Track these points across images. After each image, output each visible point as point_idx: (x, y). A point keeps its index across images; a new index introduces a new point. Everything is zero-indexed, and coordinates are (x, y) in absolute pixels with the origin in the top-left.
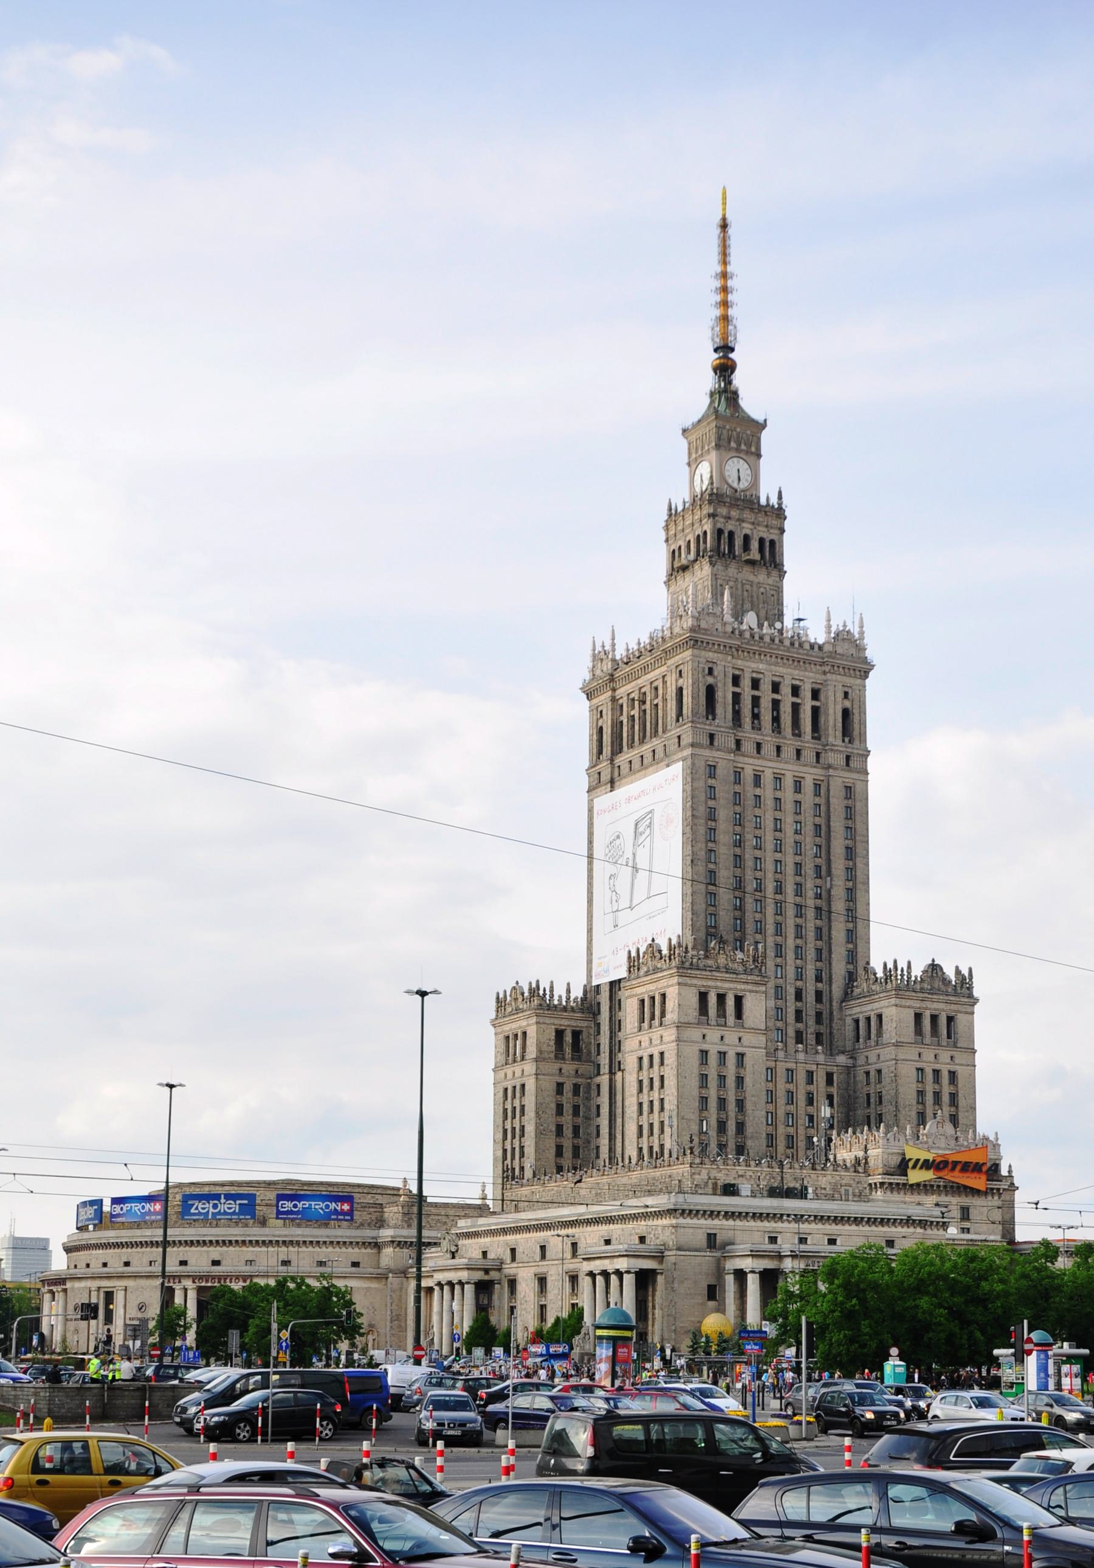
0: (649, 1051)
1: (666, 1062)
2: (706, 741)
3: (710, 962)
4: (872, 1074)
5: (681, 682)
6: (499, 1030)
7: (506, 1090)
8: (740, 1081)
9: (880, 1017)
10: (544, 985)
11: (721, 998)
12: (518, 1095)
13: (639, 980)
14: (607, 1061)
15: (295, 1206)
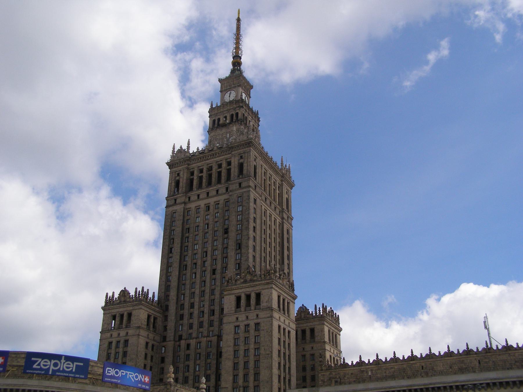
0: (246, 323)
1: (262, 328)
2: (254, 187)
3: (281, 282)
4: (308, 356)
5: (241, 161)
6: (108, 312)
7: (110, 343)
8: (289, 344)
9: (312, 330)
10: (145, 290)
11: (284, 300)
12: (121, 345)
13: (238, 286)
14: (173, 334)
15: (117, 373)
